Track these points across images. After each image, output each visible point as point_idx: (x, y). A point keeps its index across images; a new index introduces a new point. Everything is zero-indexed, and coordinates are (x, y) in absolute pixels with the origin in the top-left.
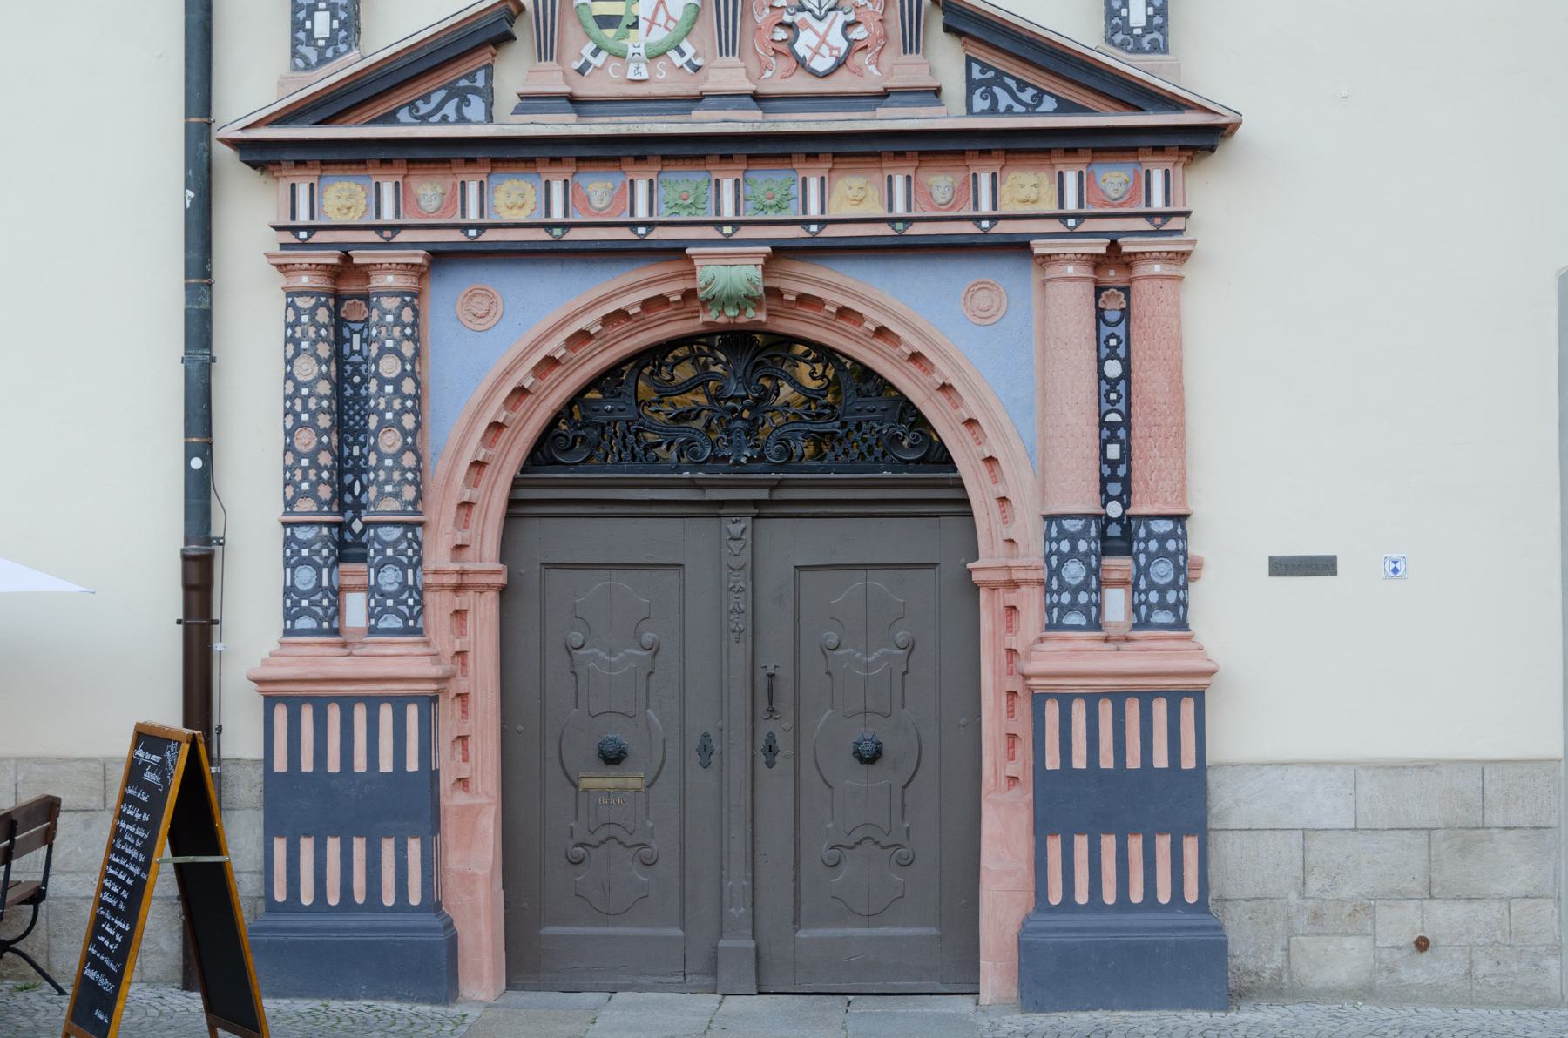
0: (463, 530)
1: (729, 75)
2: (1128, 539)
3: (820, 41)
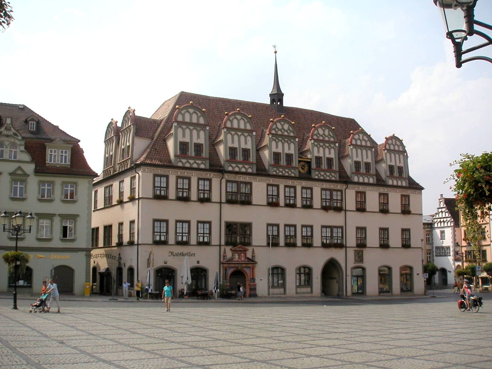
0: (228, 278)
1: (240, 260)
2: (253, 279)
3: (243, 259)
